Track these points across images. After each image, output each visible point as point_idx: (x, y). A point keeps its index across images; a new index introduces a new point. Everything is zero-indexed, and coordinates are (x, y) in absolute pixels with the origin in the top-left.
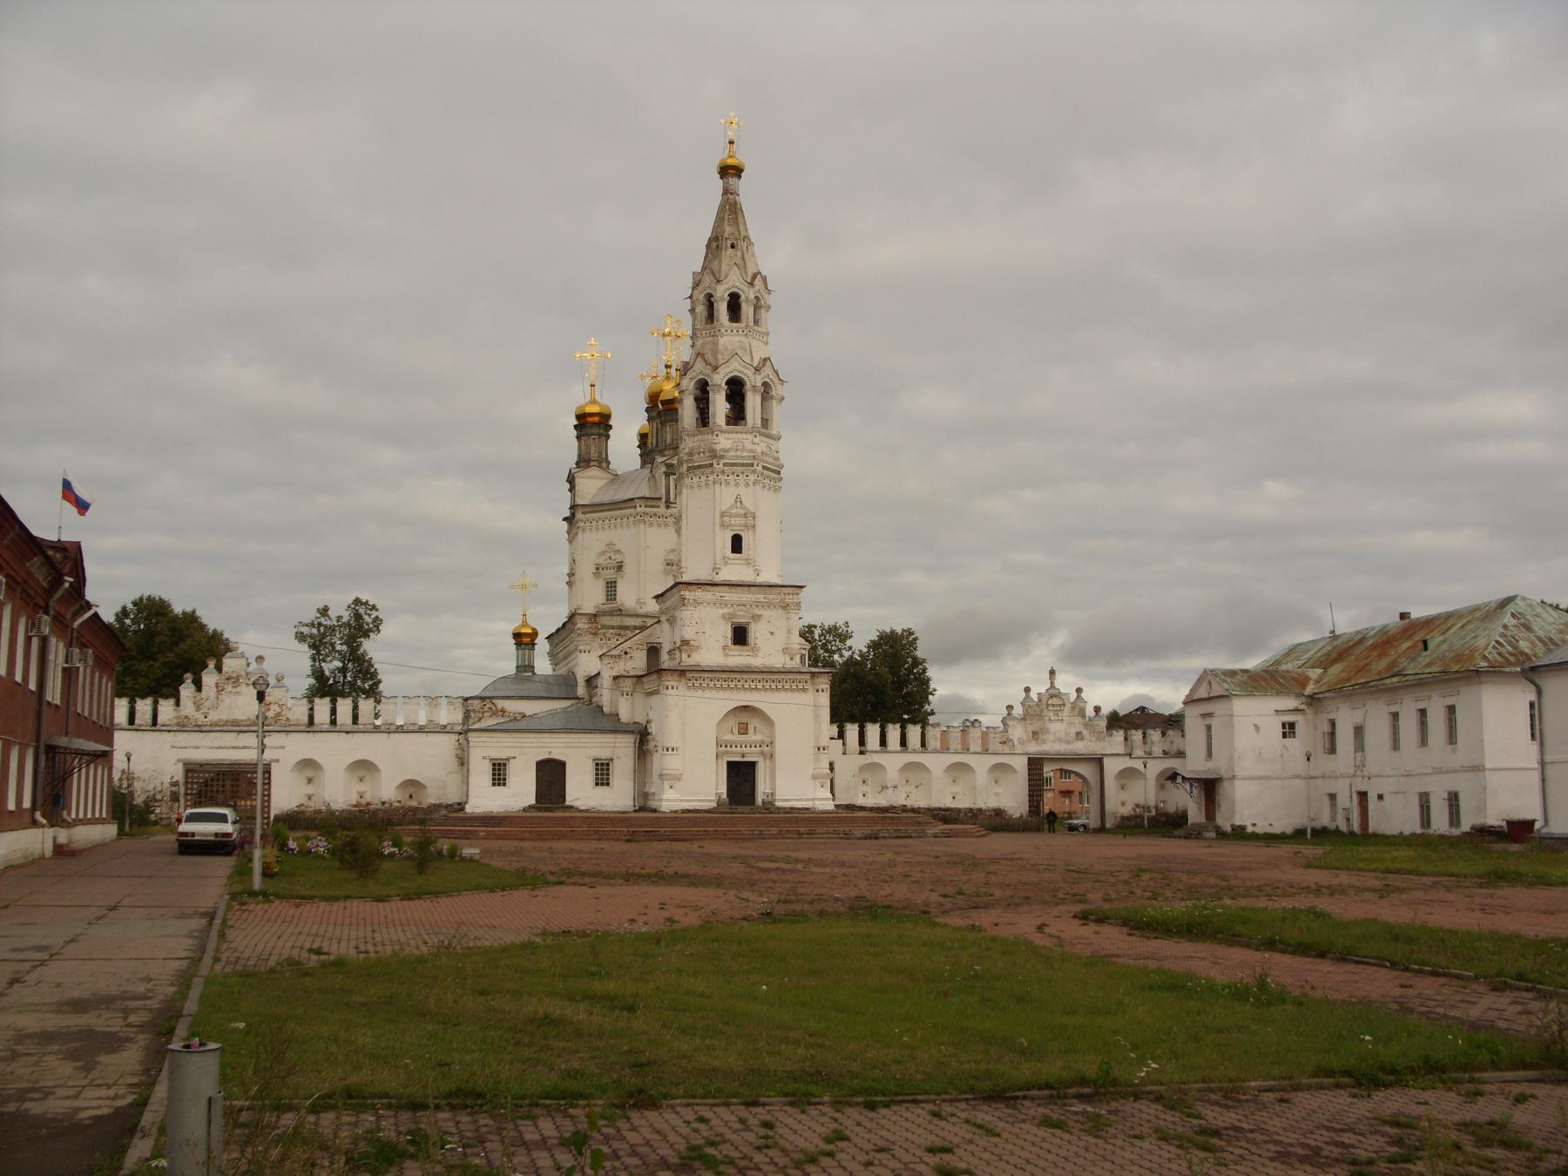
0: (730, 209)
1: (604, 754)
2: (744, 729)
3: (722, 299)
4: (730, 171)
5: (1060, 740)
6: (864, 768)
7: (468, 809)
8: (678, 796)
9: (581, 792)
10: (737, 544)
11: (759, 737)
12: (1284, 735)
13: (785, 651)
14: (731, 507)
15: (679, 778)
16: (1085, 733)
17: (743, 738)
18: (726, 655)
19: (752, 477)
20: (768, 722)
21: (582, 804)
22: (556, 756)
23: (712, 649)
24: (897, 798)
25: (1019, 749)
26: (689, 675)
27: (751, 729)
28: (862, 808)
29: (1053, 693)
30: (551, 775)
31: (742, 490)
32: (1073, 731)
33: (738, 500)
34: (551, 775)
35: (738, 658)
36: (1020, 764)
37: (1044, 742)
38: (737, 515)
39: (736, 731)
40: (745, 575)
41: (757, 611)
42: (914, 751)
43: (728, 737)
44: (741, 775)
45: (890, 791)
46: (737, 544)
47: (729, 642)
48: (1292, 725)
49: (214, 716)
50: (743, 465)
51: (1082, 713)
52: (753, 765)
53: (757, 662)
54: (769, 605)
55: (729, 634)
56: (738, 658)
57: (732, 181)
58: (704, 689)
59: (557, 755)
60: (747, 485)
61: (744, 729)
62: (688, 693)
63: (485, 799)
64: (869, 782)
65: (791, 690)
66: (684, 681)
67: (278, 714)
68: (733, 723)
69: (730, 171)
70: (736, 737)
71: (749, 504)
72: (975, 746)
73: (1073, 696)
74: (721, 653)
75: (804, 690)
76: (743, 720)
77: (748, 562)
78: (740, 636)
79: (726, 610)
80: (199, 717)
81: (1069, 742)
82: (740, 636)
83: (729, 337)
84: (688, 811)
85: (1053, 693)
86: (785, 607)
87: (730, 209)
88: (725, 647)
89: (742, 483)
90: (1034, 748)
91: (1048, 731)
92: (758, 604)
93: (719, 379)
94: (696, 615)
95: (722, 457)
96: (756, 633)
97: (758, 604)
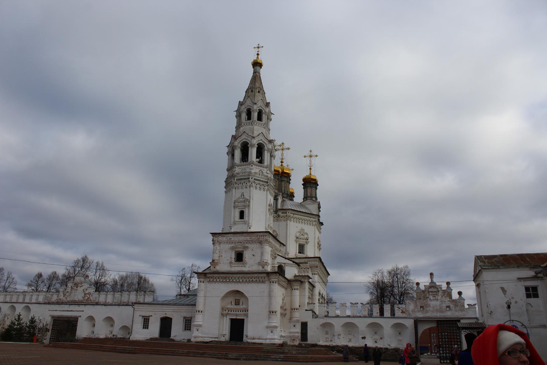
0: (256, 78)
1: (188, 315)
2: (237, 303)
4: (257, 64)
5: (437, 311)
6: (324, 325)
7: (131, 339)
8: (200, 335)
9: (177, 333)
12: (528, 296)
16: (452, 306)
17: (237, 307)
18: (231, 266)
19: (248, 184)
21: (178, 339)
25: (413, 315)
26: (208, 275)
27: (241, 303)
29: (433, 285)
30: (166, 323)
31: (244, 190)
32: (444, 305)
33: (243, 195)
34: (166, 323)
36: (409, 323)
37: (427, 312)
38: (241, 202)
39: (233, 303)
41: (247, 245)
43: (229, 306)
44: (237, 327)
47: (233, 260)
48: (535, 289)
49: (68, 299)
50: (245, 179)
51: (450, 297)
52: (243, 320)
53: (246, 269)
54: (252, 242)
55: (233, 256)
56: (238, 268)
57: (258, 68)
61: (237, 303)
62: (208, 285)
63: (139, 334)
65: (256, 282)
67: (88, 298)
68: (232, 299)
69: (257, 64)
70: (234, 306)
72: (387, 313)
73: (444, 286)
75: (263, 282)
76: (238, 298)
78: (239, 257)
79: (232, 245)
80: (64, 299)
81: (442, 312)
82: (239, 257)
83: (258, 129)
85: (433, 285)
86: (261, 243)
87: (256, 78)
88: (231, 263)
89: (244, 187)
90: (420, 315)
91: (429, 306)
92: (248, 242)
93: (238, 143)
95: (235, 176)
96: (247, 255)
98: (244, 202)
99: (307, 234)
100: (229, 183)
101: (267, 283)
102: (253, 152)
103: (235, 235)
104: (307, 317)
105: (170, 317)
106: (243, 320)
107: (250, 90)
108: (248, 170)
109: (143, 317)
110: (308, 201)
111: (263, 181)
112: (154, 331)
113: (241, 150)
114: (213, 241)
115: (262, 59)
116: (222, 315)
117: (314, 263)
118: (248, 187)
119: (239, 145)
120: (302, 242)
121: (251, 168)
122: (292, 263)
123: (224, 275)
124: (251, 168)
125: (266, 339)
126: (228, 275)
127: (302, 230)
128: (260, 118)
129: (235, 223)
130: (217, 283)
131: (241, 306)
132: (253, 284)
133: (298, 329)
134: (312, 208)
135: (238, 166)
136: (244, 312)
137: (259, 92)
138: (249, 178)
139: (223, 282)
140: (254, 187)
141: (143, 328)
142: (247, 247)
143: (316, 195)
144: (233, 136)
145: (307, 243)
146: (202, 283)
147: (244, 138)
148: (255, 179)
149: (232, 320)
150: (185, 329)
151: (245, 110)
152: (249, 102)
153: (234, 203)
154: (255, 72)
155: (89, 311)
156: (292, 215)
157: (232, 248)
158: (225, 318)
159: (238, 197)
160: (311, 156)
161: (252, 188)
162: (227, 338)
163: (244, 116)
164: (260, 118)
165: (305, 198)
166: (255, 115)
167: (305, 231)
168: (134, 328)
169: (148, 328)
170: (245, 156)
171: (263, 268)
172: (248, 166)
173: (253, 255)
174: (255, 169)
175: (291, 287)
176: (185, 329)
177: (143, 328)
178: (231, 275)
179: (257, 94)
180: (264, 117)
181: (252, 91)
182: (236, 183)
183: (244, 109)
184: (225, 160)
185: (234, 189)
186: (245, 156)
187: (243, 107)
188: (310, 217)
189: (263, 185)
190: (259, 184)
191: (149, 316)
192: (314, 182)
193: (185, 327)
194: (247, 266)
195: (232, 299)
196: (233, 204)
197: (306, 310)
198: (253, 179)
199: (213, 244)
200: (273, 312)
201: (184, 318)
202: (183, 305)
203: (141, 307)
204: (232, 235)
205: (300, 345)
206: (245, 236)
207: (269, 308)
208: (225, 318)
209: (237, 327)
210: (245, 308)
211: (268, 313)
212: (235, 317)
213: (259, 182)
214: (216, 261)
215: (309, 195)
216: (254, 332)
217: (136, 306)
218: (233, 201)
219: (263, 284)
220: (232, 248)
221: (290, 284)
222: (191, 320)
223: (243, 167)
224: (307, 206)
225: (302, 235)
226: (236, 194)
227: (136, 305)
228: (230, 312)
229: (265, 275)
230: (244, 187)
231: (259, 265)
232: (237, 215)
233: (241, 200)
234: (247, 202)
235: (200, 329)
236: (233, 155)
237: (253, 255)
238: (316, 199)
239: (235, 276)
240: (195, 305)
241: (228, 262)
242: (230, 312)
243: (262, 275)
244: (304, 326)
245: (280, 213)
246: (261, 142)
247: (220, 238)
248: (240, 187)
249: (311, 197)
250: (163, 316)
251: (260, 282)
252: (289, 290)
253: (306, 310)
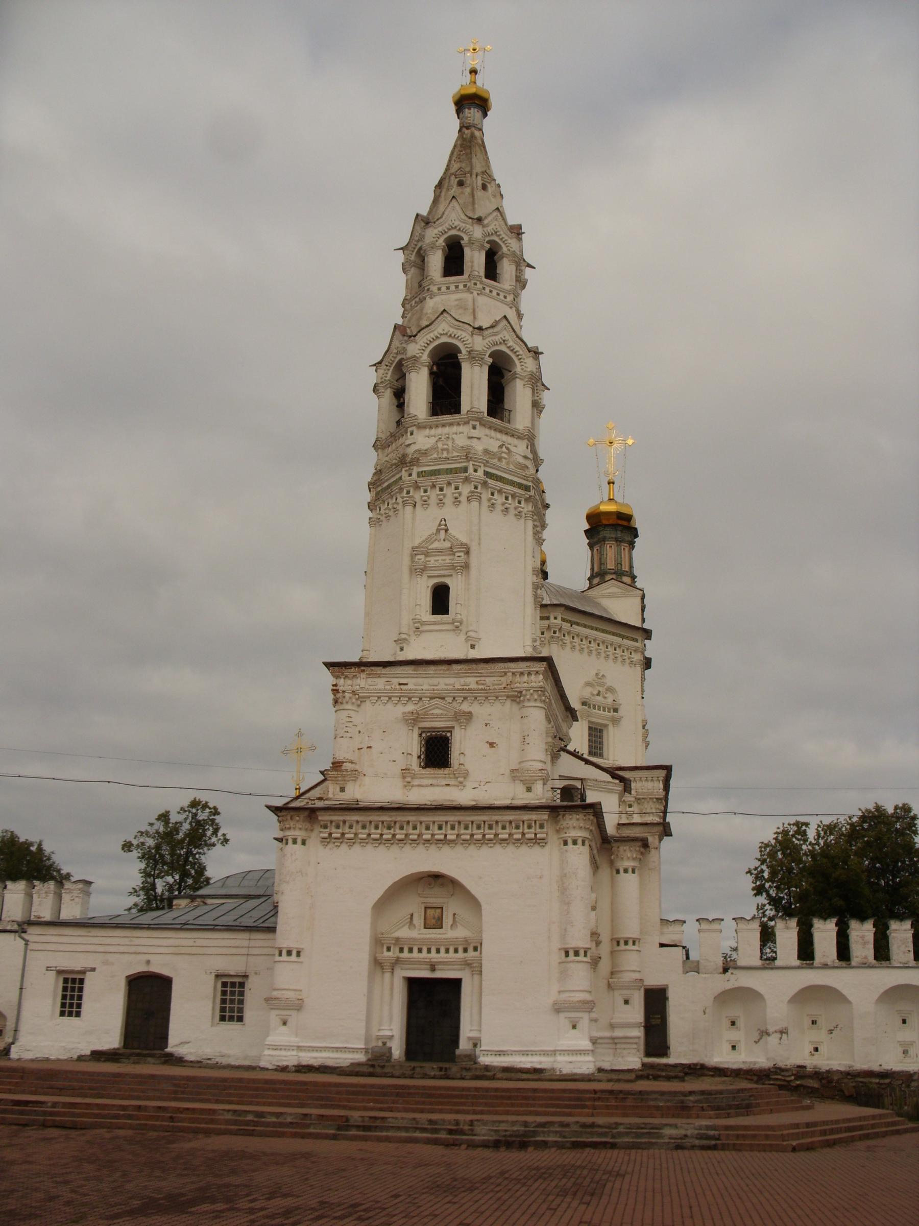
0: (469, 144)
1: (233, 966)
3: (433, 246)
6: (725, 997)
8: (294, 1040)
9: (193, 1029)
10: (440, 600)
11: (460, 933)
13: (515, 775)
14: (430, 540)
15: (298, 1006)
17: (433, 934)
18: (408, 785)
19: (466, 490)
20: (473, 903)
22: (155, 969)
24: (796, 1052)
26: (323, 817)
27: (448, 920)
28: (719, 1072)
30: (149, 998)
31: (448, 511)
34: (149, 998)
35: (432, 789)
38: (439, 552)
39: (419, 921)
40: (455, 648)
41: (465, 707)
42: (825, 966)
43: (404, 933)
45: (773, 1040)
46: (440, 600)
47: (414, 763)
50: (449, 471)
52: (456, 984)
54: (486, 695)
55: (413, 745)
56: (432, 789)
57: (473, 114)
58: (352, 842)
59: (158, 967)
60: (457, 501)
64: (741, 1022)
66: (317, 829)
69: (472, 103)
70: (418, 933)
74: (399, 783)
75: (538, 841)
77: (457, 626)
78: (436, 752)
79: (410, 707)
82: (436, 752)
84: (309, 1069)
87: (469, 144)
88: (405, 771)
89: (449, 500)
92: (467, 694)
93: (420, 350)
94: (357, 718)
95: (415, 462)
96: (465, 745)
97: (467, 694)
98: (451, 551)
99: (610, 690)
100: (384, 490)
101: (554, 841)
103: (421, 670)
104: (661, 969)
105: (165, 972)
106: (456, 984)
107: (454, 181)
108: (461, 441)
109: (60, 972)
110: (611, 587)
111: (512, 483)
112: (103, 1022)
113: (431, 373)
114: (335, 691)
115: (486, 83)
116: (377, 964)
117: (650, 785)
118: (463, 499)
119: (425, 358)
121: (475, 433)
122: (607, 777)
123: (386, 817)
124: (475, 433)
125: (554, 1052)
126: (400, 817)
127: (599, 677)
128: (491, 272)
129: (418, 628)
130: (357, 848)
131: (448, 933)
132: (498, 849)
133: (636, 1013)
134: (623, 608)
135: (420, 427)
136: (461, 954)
137: (484, 187)
138: (465, 470)
139: (380, 841)
140: (485, 503)
141: (62, 1014)
142: (469, 716)
143: (631, 567)
144: (396, 327)
145: (616, 721)
146: (299, 846)
147: (442, 333)
148: (486, 474)
149: (413, 984)
150: (223, 1018)
151: (441, 242)
152: (453, 218)
153: (413, 556)
156: (566, 626)
157: (413, 720)
158: (387, 975)
159: (426, 534)
161: (475, 504)
163: (436, 261)
164: (491, 272)
165: (598, 576)
166: (475, 260)
167: (609, 682)
168: (25, 1014)
169: (78, 1014)
170: (446, 398)
171: (529, 790)
172: (461, 428)
173: (492, 745)
174: (486, 440)
175: (612, 863)
176: (223, 1018)
177: (62, 1014)
178: (412, 818)
179: (479, 194)
180: (506, 268)
181: (461, 184)
182: (417, 487)
183: (435, 237)
184: (369, 412)
185: (409, 509)
186: (446, 398)
187: (431, 234)
188: (623, 637)
189: (514, 496)
190: (500, 492)
191: (83, 972)
192: (625, 523)
193: (223, 1010)
194: (469, 784)
195: (413, 905)
196: (406, 561)
197: (662, 945)
198: (480, 473)
199: (336, 702)
200: (577, 953)
201: (218, 976)
202: (214, 928)
203: (53, 936)
204: (409, 669)
205: (647, 1072)
206: (458, 676)
207: (612, 933)
208: (387, 975)
209: (434, 1005)
210: (466, 941)
211: (559, 956)
212: (424, 973)
213: (500, 484)
214: (347, 766)
215: (611, 565)
216: (506, 1027)
217: (33, 934)
218: (407, 552)
219: (537, 849)
221: (610, 852)
222: (242, 985)
223: (440, 430)
224: (605, 602)
225: (598, 694)
226: (418, 523)
227: (32, 930)
228: (406, 954)
229: (544, 816)
230: (449, 500)
231: (514, 779)
232: (426, 600)
233: (436, 545)
234: (462, 556)
235: (294, 1018)
236: (400, 394)
237: (492, 745)
238: (634, 578)
239: (427, 818)
240: (272, 930)
241: (397, 769)
242: (406, 954)
243: (534, 816)
244: (656, 1001)
246: (503, 348)
247: (363, 682)
248: (433, 500)
249: (619, 574)
250: (142, 968)
251: (523, 841)
252: (605, 873)
253: (662, 945)
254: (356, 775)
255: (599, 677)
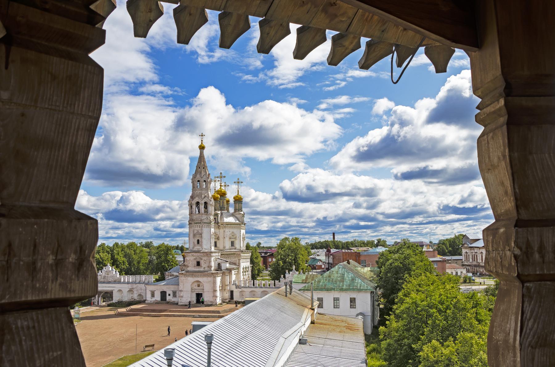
23: (192, 267)
30: (163, 294)
35: (197, 269)
44: (199, 296)
53: (202, 269)
55: (196, 263)
56: (197, 269)
61: (199, 286)
68: (196, 284)
70: (197, 287)
71: (200, 231)
78: (198, 264)
82: (198, 264)
96: (202, 263)
102: (202, 207)
104: (233, 288)
112: (158, 297)
120: (232, 240)
127: (233, 232)
147: (197, 199)
154: (201, 152)
155: (118, 286)
160: (238, 182)
162: (195, 302)
174: (204, 217)
215: (237, 208)
220: (195, 259)
232: (196, 242)
244: (232, 292)
245: (220, 224)
254: (188, 267)
255: (233, 232)
